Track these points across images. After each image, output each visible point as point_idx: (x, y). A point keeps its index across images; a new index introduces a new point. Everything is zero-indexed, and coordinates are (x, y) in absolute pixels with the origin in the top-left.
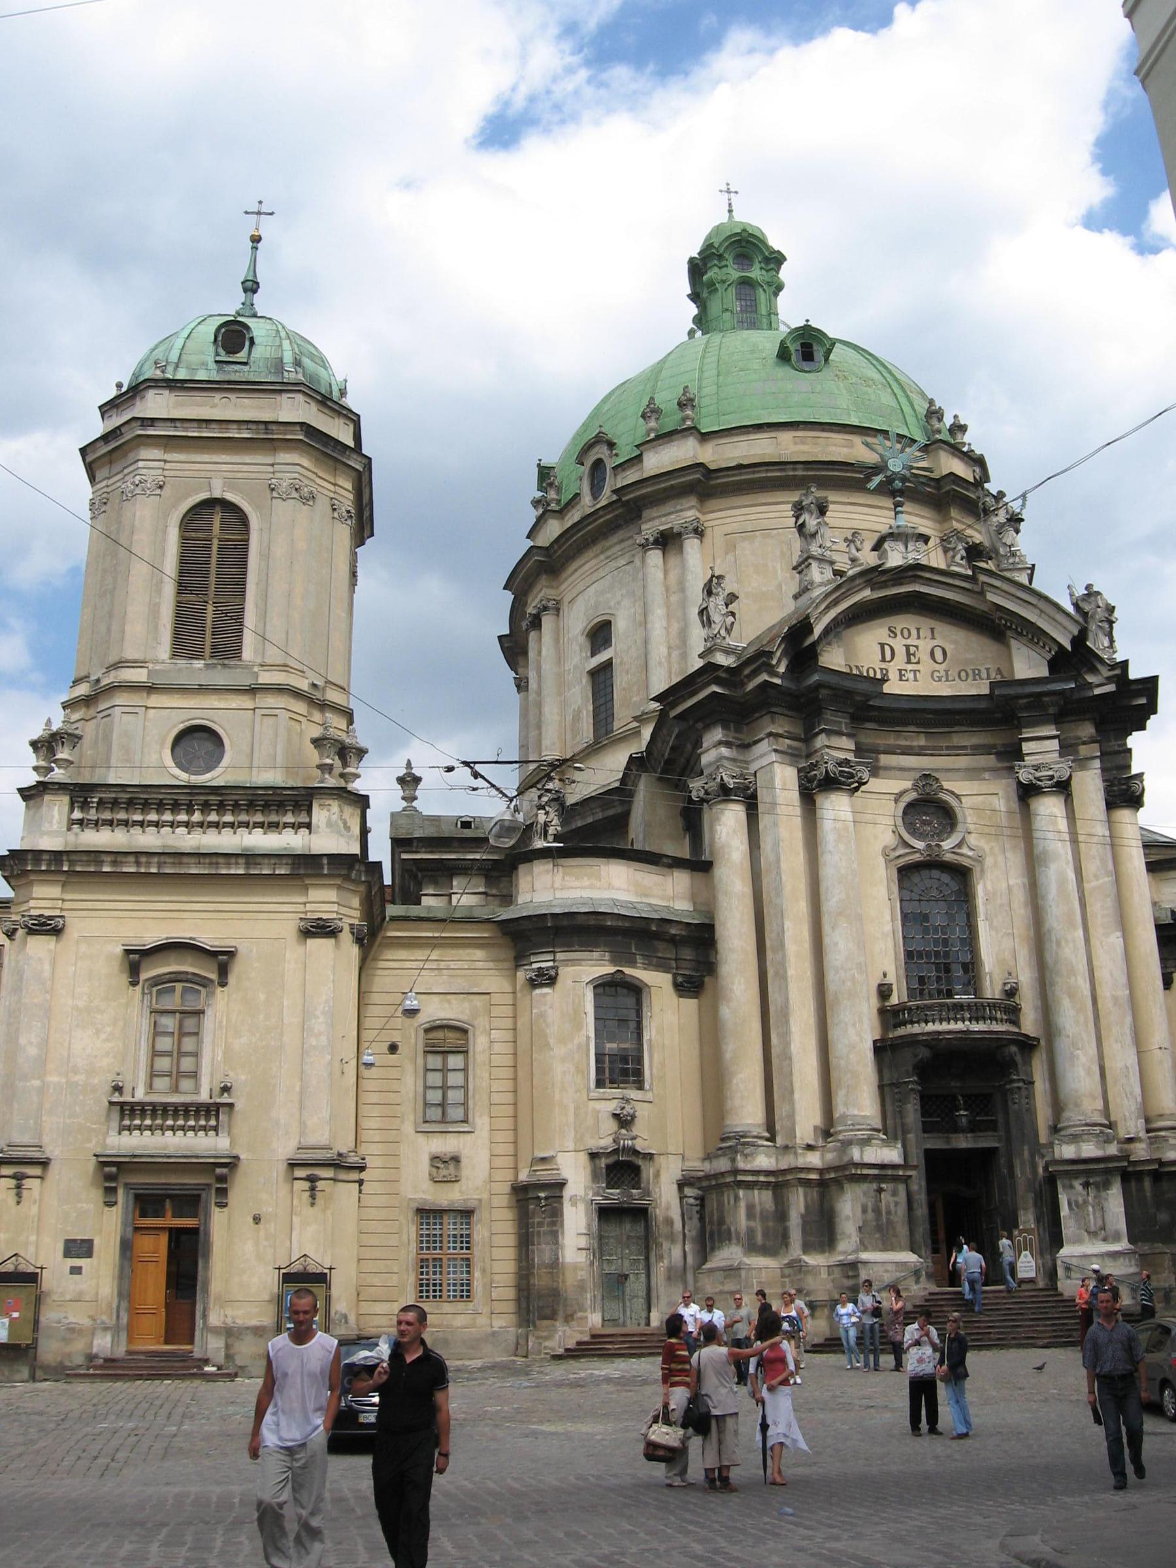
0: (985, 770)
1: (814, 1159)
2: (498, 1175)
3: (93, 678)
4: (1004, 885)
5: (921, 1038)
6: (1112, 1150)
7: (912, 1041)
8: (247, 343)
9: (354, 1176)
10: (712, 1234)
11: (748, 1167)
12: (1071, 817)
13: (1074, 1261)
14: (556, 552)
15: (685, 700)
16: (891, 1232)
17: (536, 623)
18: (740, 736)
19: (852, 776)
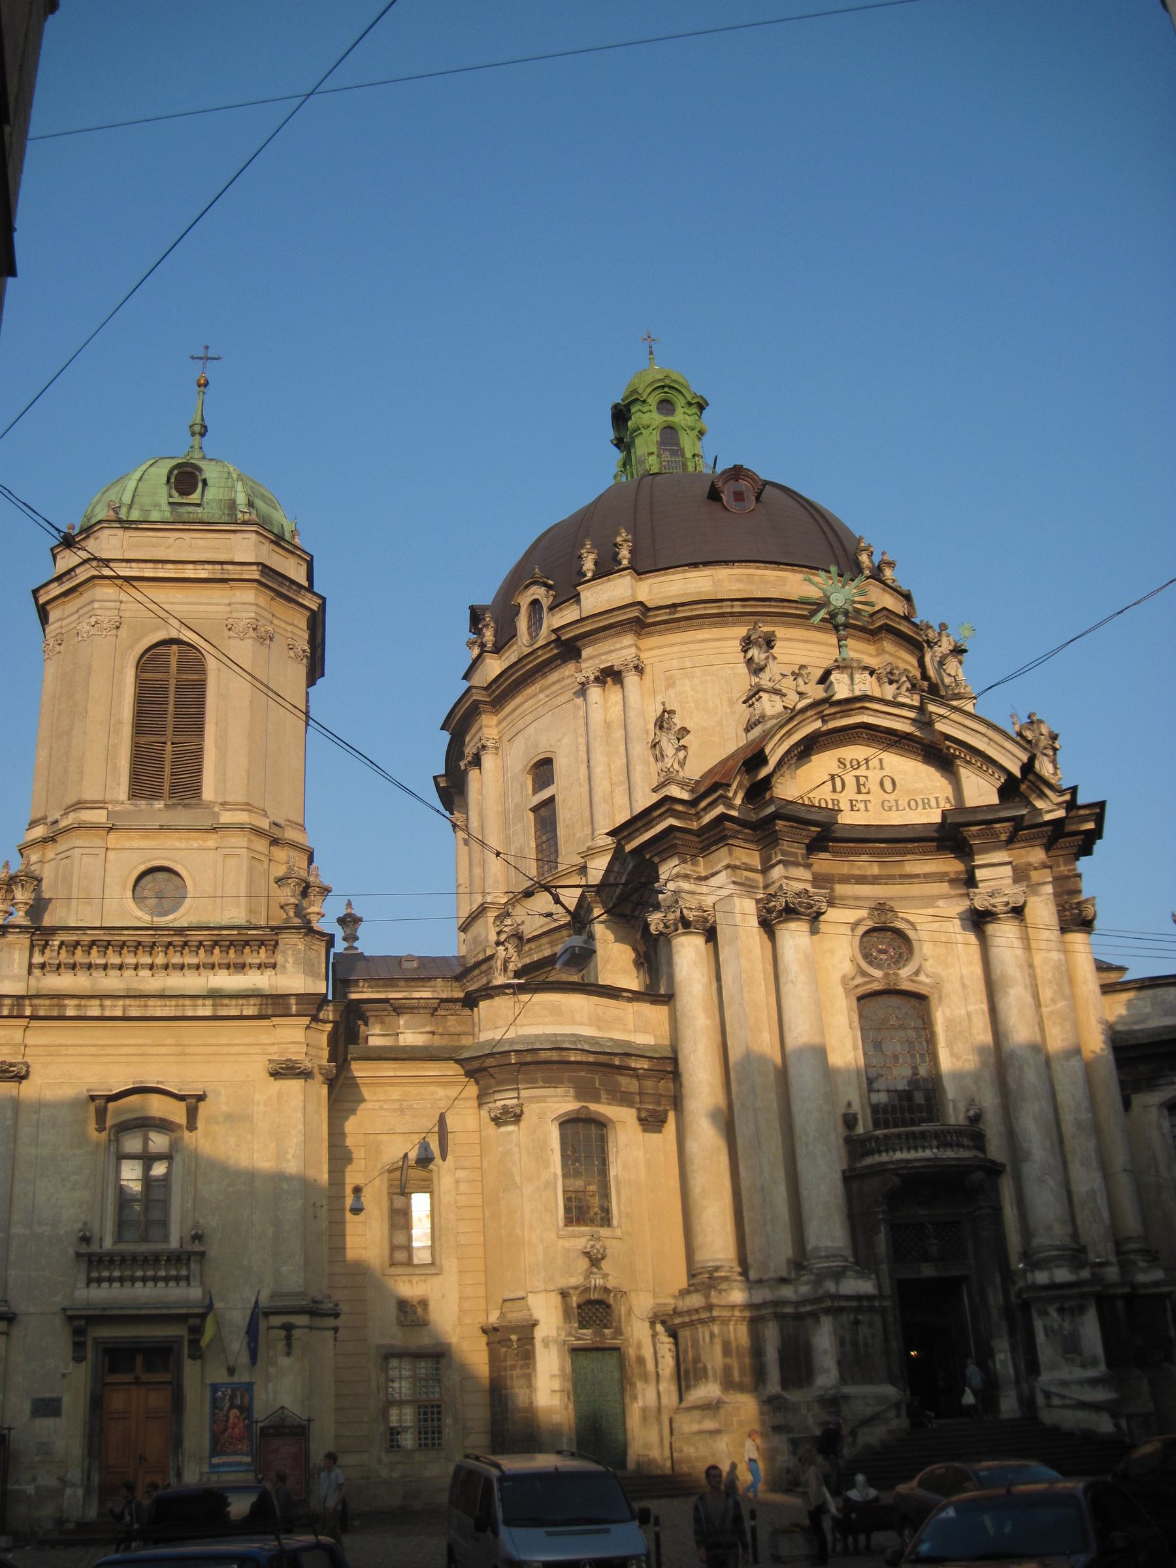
1: (787, 1292)
2: (467, 1320)
3: (50, 820)
4: (963, 1012)
6: (1085, 1274)
7: (879, 1170)
8: (200, 485)
9: (330, 1322)
10: (687, 1372)
11: (723, 1303)
12: (1026, 941)
13: (1053, 1389)
14: (494, 691)
15: (641, 834)
17: (477, 762)
18: (697, 869)
19: (811, 906)
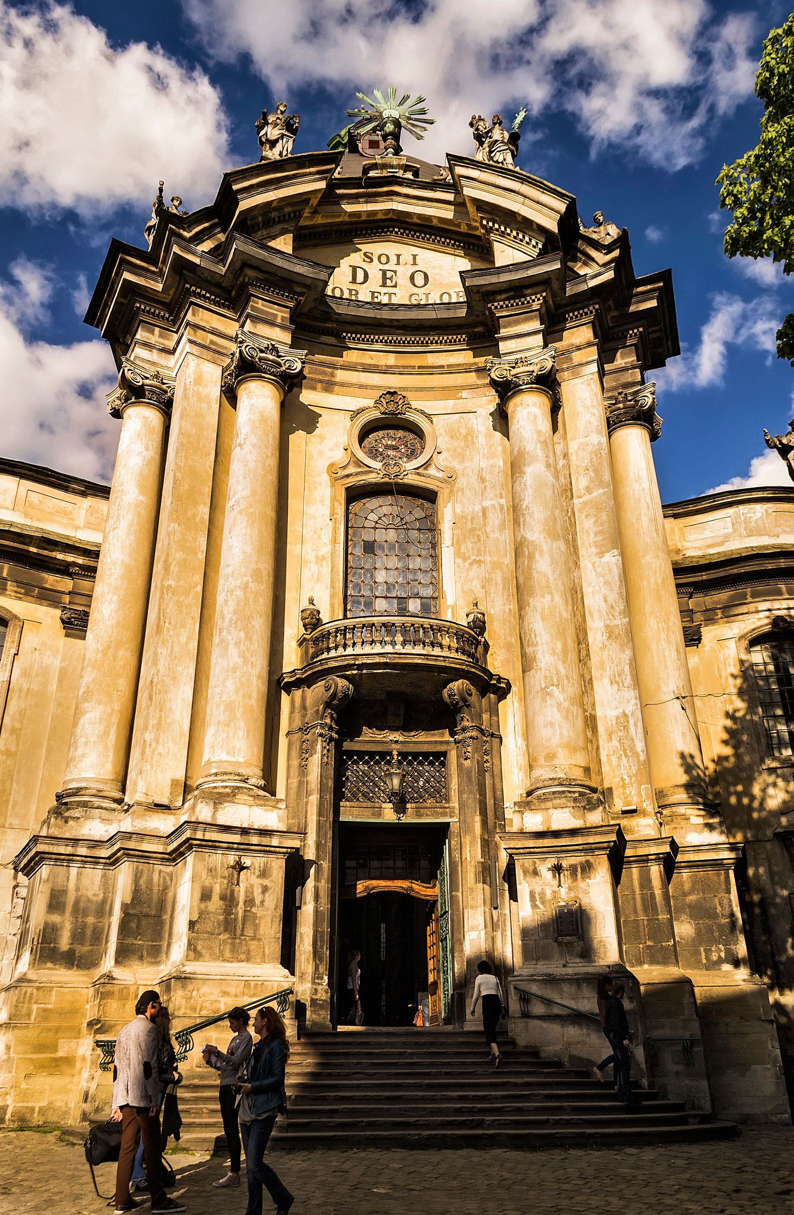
0: (463, 388)
1: (165, 824)
4: (478, 508)
5: (333, 664)
11: (68, 835)
13: (534, 989)
16: (249, 932)
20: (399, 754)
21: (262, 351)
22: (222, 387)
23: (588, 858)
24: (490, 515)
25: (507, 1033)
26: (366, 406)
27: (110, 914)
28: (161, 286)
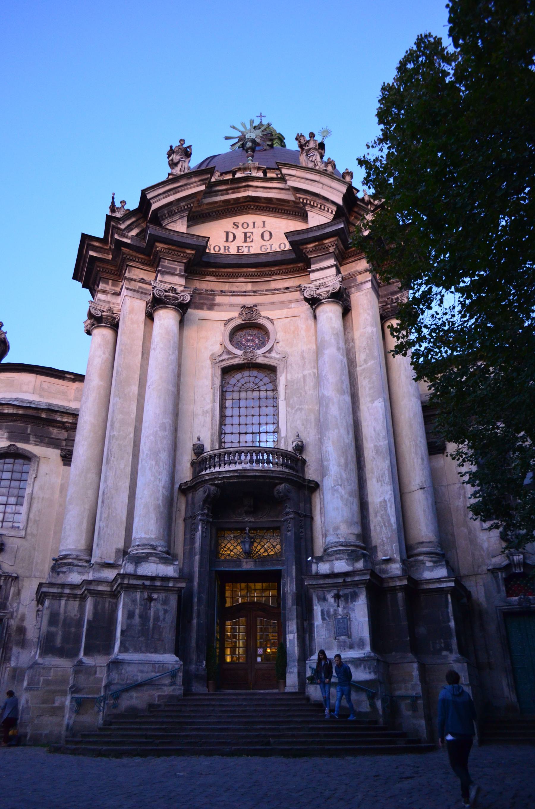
4: (300, 375)
5: (207, 478)
11: (59, 582)
19: (177, 299)
20: (251, 529)
21: (166, 291)
22: (146, 313)
23: (355, 589)
24: (308, 380)
25: (304, 693)
26: (234, 317)
27: (83, 627)
28: (111, 256)
